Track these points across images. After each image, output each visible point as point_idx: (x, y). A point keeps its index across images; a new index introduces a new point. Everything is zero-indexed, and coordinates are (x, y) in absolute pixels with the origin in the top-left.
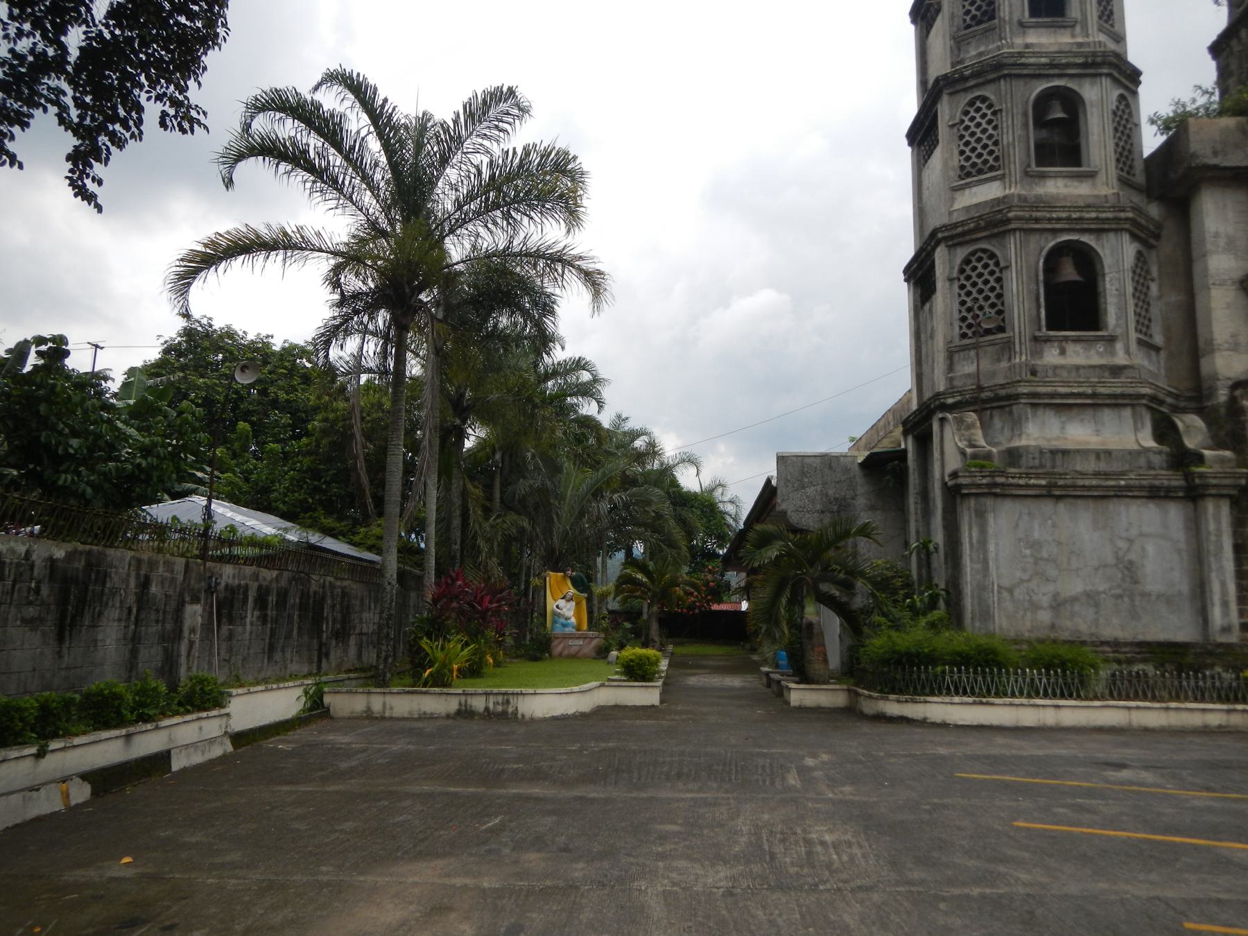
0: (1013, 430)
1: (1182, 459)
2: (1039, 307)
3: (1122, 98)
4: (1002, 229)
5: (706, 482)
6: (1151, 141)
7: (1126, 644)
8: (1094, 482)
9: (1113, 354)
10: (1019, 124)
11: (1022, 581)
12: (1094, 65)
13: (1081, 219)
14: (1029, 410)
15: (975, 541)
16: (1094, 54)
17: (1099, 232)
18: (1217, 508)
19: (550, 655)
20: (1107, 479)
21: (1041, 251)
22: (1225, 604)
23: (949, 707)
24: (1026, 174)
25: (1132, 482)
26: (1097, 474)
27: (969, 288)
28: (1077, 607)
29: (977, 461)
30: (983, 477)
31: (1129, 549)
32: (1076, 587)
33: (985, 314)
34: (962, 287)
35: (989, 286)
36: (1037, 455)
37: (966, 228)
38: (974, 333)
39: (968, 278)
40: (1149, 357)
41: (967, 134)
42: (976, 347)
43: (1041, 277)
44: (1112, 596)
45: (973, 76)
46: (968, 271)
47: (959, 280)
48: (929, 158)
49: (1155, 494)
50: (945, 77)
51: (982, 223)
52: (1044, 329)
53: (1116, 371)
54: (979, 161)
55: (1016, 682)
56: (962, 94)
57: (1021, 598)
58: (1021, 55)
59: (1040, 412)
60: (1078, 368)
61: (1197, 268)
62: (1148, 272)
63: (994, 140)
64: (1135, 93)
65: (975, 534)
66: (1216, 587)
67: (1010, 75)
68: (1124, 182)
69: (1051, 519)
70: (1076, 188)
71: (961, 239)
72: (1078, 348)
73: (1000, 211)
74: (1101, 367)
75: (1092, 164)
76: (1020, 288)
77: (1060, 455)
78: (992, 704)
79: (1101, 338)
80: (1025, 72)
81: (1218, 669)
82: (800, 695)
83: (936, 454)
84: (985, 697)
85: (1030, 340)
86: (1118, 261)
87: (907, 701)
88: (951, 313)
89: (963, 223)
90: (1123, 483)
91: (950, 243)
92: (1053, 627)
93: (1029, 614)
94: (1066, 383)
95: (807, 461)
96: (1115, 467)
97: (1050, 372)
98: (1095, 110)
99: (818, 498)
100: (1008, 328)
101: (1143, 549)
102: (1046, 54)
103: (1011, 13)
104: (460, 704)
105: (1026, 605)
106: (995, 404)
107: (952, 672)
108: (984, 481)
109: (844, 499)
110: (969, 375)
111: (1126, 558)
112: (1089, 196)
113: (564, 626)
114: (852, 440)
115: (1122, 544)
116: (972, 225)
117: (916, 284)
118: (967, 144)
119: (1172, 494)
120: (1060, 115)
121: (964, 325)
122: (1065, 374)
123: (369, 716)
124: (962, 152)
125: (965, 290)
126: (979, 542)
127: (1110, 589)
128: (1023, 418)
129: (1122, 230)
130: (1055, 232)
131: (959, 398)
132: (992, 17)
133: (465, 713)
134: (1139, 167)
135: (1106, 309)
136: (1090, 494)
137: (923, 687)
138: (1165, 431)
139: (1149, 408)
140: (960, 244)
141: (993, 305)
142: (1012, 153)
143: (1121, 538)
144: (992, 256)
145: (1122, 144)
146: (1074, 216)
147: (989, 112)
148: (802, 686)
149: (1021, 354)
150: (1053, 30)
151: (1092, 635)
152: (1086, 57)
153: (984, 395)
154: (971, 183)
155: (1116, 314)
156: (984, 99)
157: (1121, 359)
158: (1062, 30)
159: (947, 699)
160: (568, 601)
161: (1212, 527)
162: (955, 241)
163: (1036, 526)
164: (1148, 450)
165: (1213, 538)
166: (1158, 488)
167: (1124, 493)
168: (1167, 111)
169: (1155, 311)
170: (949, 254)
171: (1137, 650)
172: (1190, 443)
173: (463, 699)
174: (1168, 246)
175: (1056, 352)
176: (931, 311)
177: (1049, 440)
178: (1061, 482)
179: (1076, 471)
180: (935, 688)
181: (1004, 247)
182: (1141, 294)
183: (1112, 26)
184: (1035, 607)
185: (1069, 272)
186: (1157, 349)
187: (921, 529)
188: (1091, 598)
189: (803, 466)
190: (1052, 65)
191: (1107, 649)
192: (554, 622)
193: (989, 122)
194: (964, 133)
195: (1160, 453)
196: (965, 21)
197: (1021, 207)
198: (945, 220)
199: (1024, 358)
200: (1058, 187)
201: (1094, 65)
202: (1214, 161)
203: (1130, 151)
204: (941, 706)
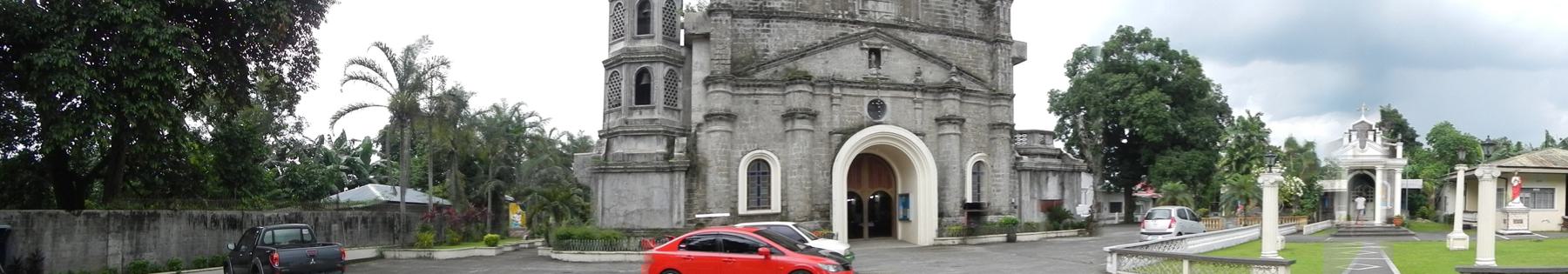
18: (680, 175)
22: (679, 213)
49: (659, 171)
66: (676, 207)
101: (653, 192)
161: (677, 183)
166: (659, 168)
202: (693, 32)
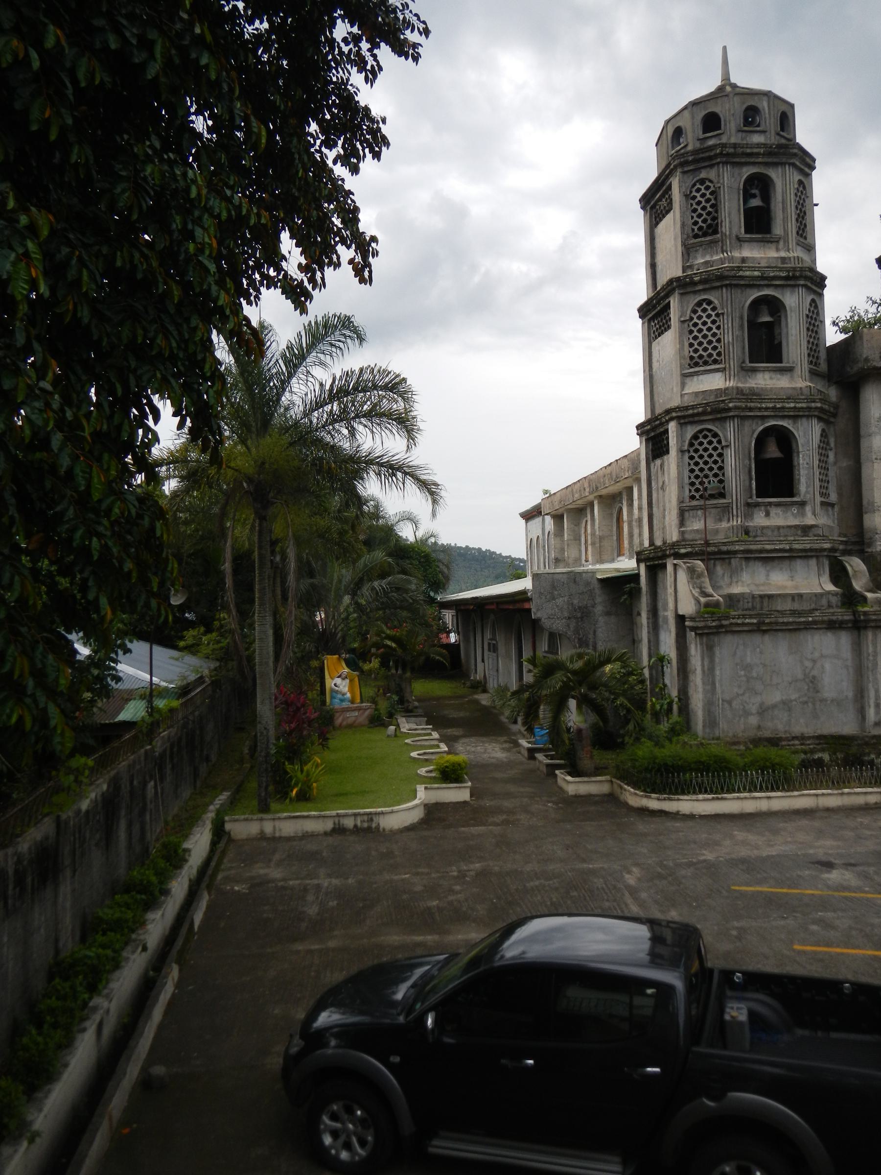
0: (731, 577)
1: (851, 598)
2: (751, 479)
3: (813, 301)
4: (724, 415)
5: (420, 534)
6: (833, 336)
7: (809, 738)
8: (791, 620)
9: (803, 514)
10: (737, 325)
11: (738, 695)
12: (794, 278)
13: (783, 408)
14: (744, 563)
15: (706, 668)
16: (794, 269)
17: (795, 418)
19: (334, 727)
20: (800, 617)
21: (753, 433)
23: (696, 803)
24: (742, 369)
25: (817, 618)
26: (793, 613)
27: (697, 459)
28: (776, 712)
29: (709, 609)
30: (713, 621)
31: (813, 668)
32: (776, 697)
33: (709, 483)
34: (692, 458)
35: (713, 459)
36: (750, 600)
37: (695, 411)
38: (701, 496)
39: (696, 451)
40: (827, 511)
41: (695, 330)
42: (703, 508)
43: (753, 456)
44: (800, 703)
45: (701, 282)
46: (697, 446)
47: (689, 451)
48: (659, 336)
49: (833, 626)
50: (678, 279)
51: (709, 409)
52: (754, 497)
53: (806, 529)
54: (705, 354)
55: (741, 782)
56: (692, 296)
57: (737, 707)
58: (739, 269)
59: (751, 563)
60: (779, 528)
61: (864, 444)
62: (828, 444)
63: (717, 337)
64: (821, 295)
65: (706, 663)
67: (730, 285)
68: (814, 374)
69: (759, 647)
70: (778, 380)
71: (691, 419)
72: (779, 510)
73: (723, 401)
74: (796, 527)
75: (791, 361)
76: (737, 464)
77: (767, 599)
78: (725, 799)
79: (793, 504)
80: (742, 282)
81: (873, 756)
82: (572, 785)
83: (670, 590)
84: (720, 794)
85: (744, 505)
86: (808, 441)
87: (665, 799)
88: (683, 479)
89: (693, 407)
90: (810, 619)
91: (682, 421)
92: (759, 728)
93: (742, 719)
94: (771, 542)
95: (556, 576)
96: (806, 606)
97: (759, 532)
98: (793, 314)
99: (565, 607)
100: (727, 494)
101: (823, 667)
102: (759, 269)
103: (730, 229)
104: (334, 823)
105: (741, 712)
106: (717, 557)
107: (697, 777)
108: (714, 624)
109: (586, 607)
110: (697, 531)
111: (812, 674)
112: (788, 388)
113: (342, 700)
114: (546, 492)
115: (808, 664)
116: (700, 410)
117: (647, 440)
118: (695, 338)
119: (844, 626)
120: (767, 319)
121: (693, 489)
122: (770, 533)
123: (262, 836)
124: (691, 345)
125: (694, 461)
126: (709, 669)
127: (799, 697)
128: (739, 569)
129: (812, 416)
130: (763, 418)
131: (689, 550)
132: (715, 232)
133: (339, 830)
134: (823, 355)
135: (799, 480)
136: (787, 628)
137: (676, 789)
138: (839, 575)
139: (827, 556)
140: (692, 423)
141: (716, 475)
142: (731, 351)
143: (807, 659)
144: (715, 435)
145: (811, 340)
146: (778, 406)
147: (713, 314)
148: (577, 779)
149: (737, 517)
150: (762, 244)
151: (786, 732)
152: (788, 271)
153: (710, 549)
154: (699, 371)
155: (807, 483)
156: (709, 302)
157: (810, 520)
158: (770, 245)
159: (694, 797)
160: (343, 679)
161: (871, 649)
162: (686, 420)
163: (749, 653)
164: (829, 593)
165: (871, 658)
166: (834, 622)
167: (811, 626)
168: (844, 314)
169: (832, 473)
170: (681, 429)
171: (817, 742)
172: (858, 585)
173: (336, 820)
174: (842, 422)
175: (762, 514)
176: (662, 465)
177: (757, 585)
178: (767, 621)
179: (778, 611)
180: (684, 789)
181: (725, 429)
182: (824, 466)
183: (805, 238)
184: (747, 713)
185: (773, 451)
186: (832, 505)
187: (652, 639)
188: (786, 705)
189: (553, 581)
190: (762, 278)
191: (797, 742)
192: (332, 697)
193: (714, 322)
194: (693, 328)
195: (835, 594)
196: (693, 230)
197: (739, 399)
198: (676, 402)
199: (739, 521)
200: (765, 380)
201: (794, 278)
203: (817, 345)
204: (690, 802)
